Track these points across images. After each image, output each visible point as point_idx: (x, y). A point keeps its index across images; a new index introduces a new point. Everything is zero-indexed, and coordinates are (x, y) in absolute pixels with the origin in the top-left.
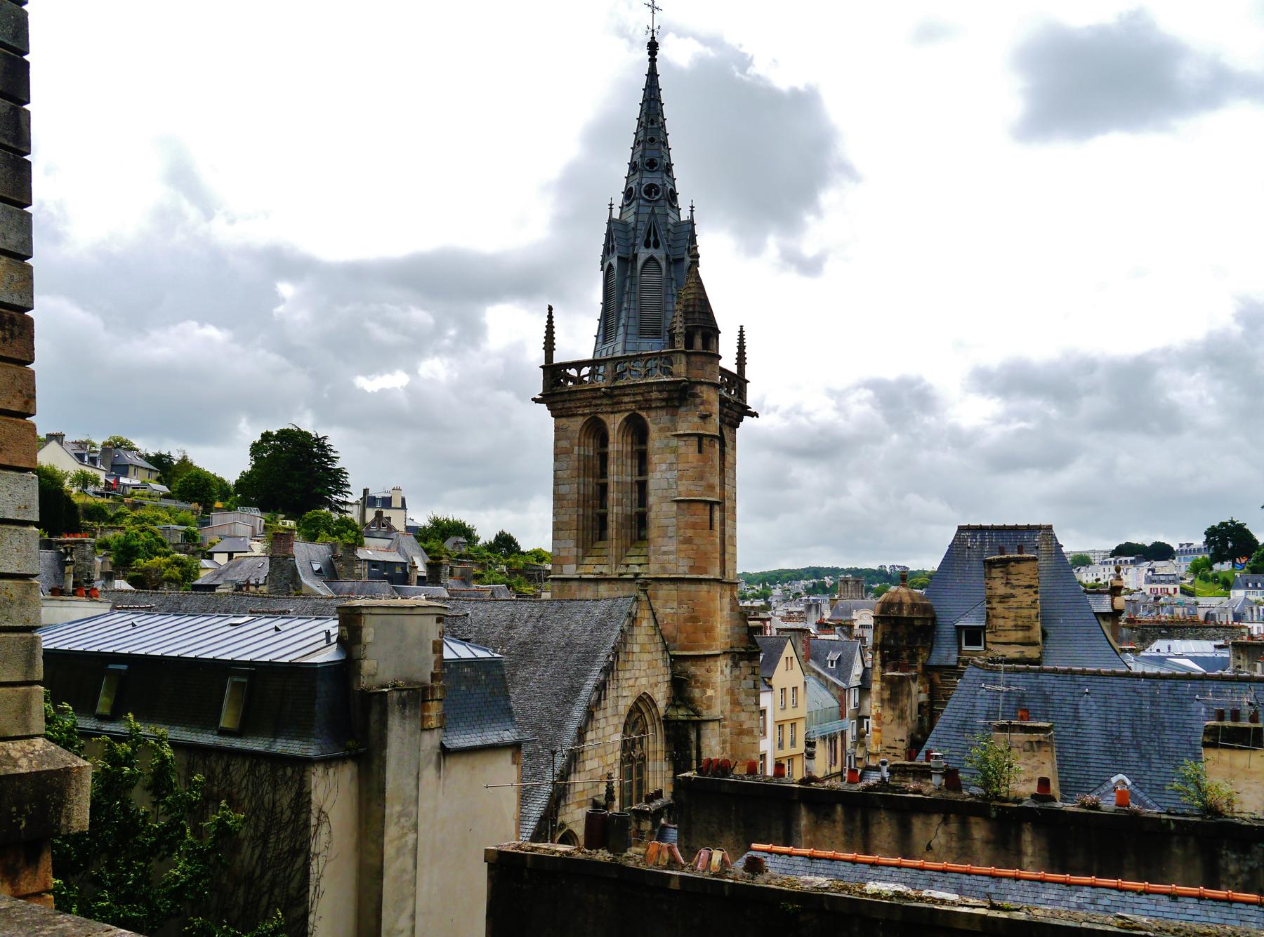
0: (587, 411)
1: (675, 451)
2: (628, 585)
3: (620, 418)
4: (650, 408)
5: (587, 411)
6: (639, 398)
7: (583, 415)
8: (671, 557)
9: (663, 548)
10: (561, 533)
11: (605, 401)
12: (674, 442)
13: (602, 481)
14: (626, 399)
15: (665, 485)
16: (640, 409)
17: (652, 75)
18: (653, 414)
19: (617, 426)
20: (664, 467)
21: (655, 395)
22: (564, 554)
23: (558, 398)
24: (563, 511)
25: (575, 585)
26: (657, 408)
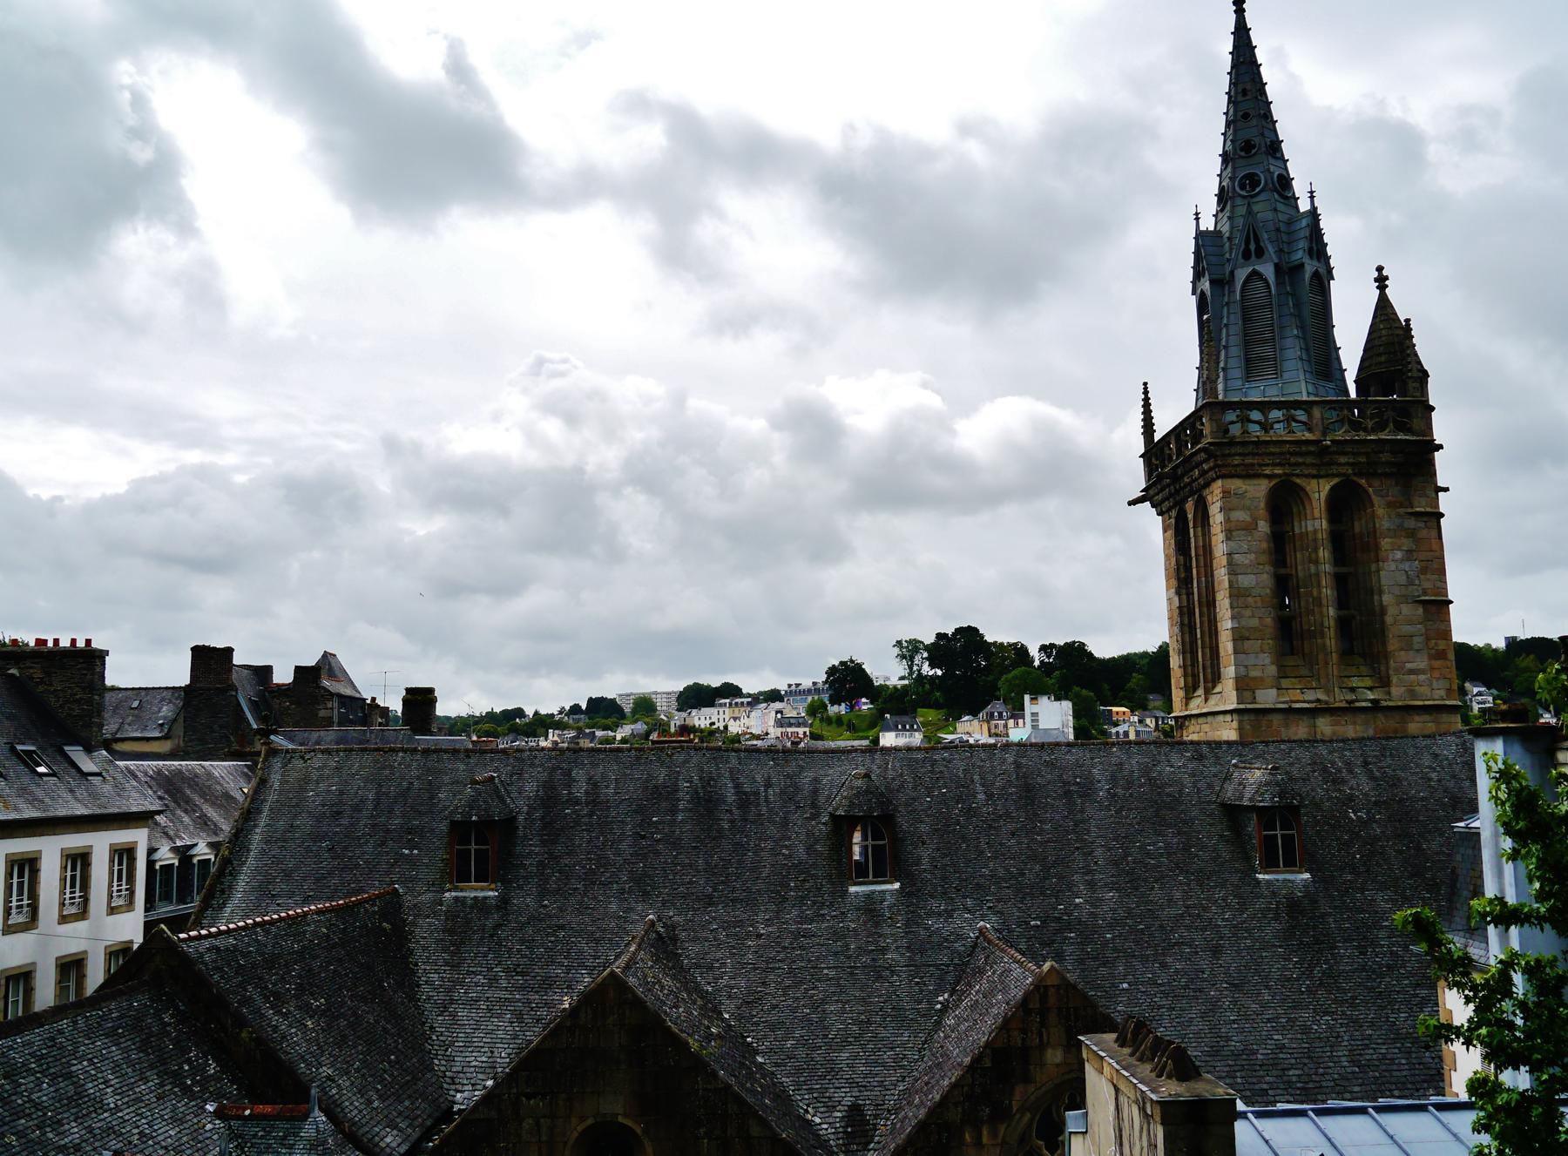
0: (1278, 471)
1: (1411, 534)
2: (1361, 718)
3: (1326, 487)
4: (1375, 475)
5: (1278, 471)
6: (1363, 459)
7: (1267, 476)
8: (1422, 677)
9: (1409, 666)
10: (1247, 644)
11: (1309, 460)
12: (1411, 523)
13: (1343, 570)
14: (1343, 460)
15: (1403, 579)
16: (1360, 475)
17: (1241, 33)
18: (1376, 483)
19: (1323, 495)
20: (1399, 555)
21: (1385, 457)
22: (1253, 674)
23: (1239, 450)
24: (1248, 612)
25: (1276, 720)
26: (1386, 475)
